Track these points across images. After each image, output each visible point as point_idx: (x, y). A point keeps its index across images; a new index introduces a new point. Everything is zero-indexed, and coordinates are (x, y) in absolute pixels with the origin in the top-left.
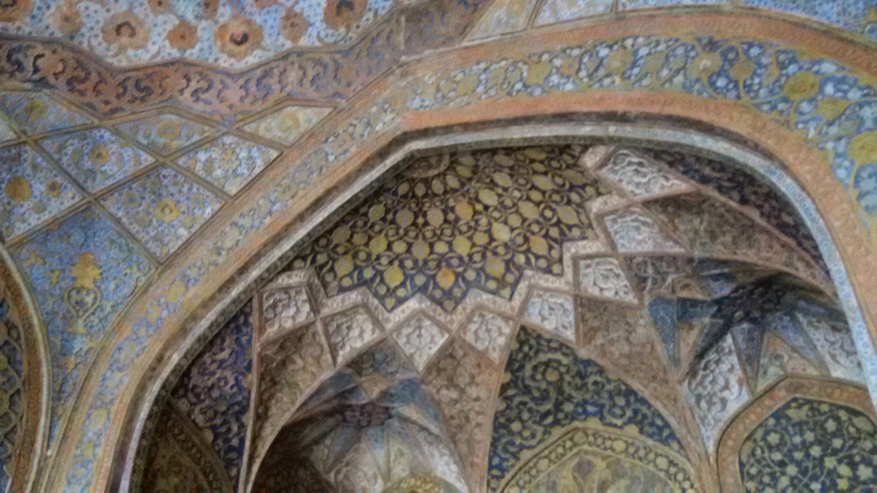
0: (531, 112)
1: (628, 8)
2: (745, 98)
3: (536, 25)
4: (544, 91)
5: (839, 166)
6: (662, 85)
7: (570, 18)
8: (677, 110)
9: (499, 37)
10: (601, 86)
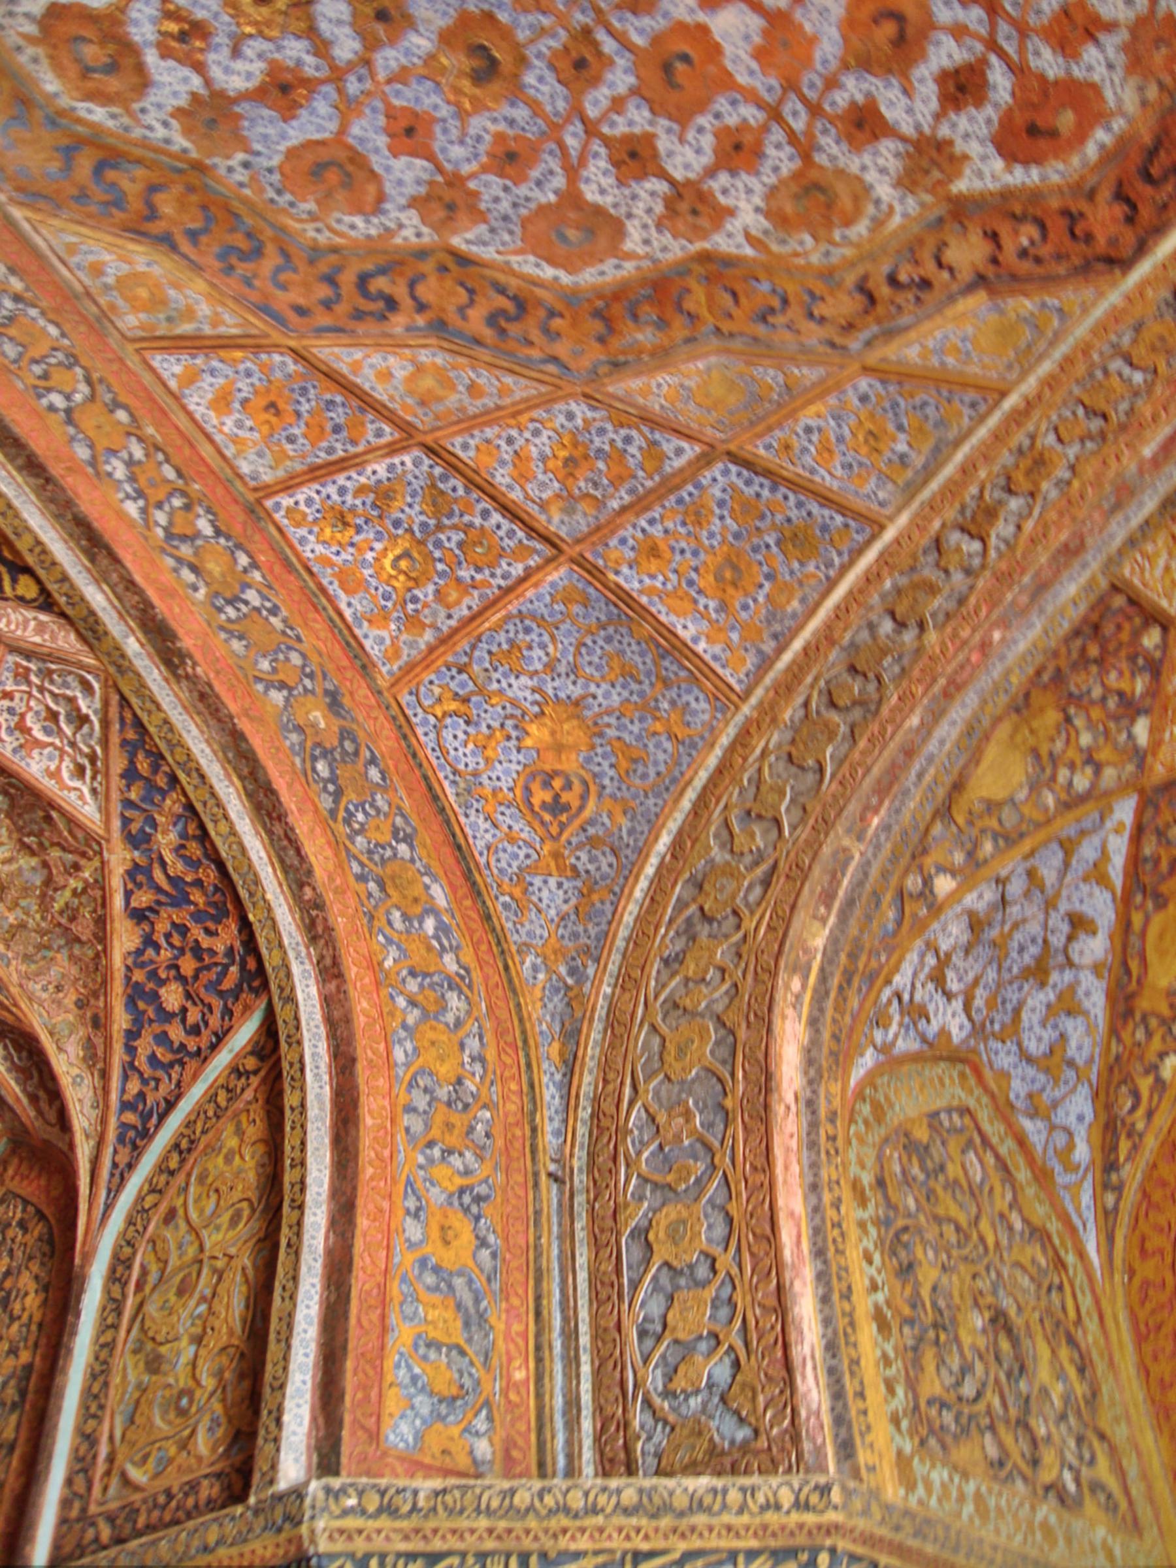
0: (56, 470)
1: (278, 516)
2: (342, 829)
3: (147, 355)
4: (93, 462)
5: (400, 1042)
6: (258, 679)
7: (198, 417)
8: (258, 743)
9: (79, 288)
10: (176, 570)
